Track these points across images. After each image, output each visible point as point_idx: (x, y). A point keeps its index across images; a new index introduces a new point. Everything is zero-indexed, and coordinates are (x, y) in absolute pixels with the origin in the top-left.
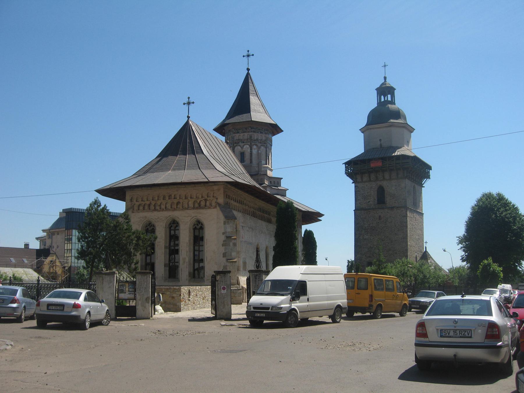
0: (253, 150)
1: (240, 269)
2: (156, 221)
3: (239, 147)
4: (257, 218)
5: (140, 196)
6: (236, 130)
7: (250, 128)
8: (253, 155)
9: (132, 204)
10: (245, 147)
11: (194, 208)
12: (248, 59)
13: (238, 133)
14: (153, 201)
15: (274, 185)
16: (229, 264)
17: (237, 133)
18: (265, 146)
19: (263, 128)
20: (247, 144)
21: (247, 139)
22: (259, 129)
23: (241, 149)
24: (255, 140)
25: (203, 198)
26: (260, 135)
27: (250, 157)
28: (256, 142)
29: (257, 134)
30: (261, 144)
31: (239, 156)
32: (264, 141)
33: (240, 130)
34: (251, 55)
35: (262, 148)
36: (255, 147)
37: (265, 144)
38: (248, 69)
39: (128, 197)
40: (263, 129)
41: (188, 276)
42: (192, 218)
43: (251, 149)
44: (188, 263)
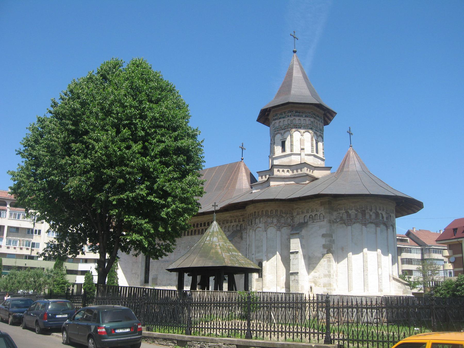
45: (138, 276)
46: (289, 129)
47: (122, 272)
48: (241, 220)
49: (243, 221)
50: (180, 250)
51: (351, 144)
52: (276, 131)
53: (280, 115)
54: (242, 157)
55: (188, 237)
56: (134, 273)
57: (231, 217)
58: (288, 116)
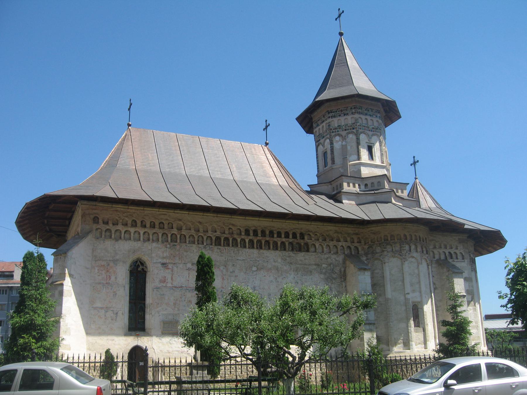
0: (335, 144)
15: (373, 188)
17: (317, 126)
18: (354, 132)
22: (342, 111)
24: (336, 129)
26: (342, 118)
28: (338, 131)
29: (339, 118)
30: (347, 131)
31: (322, 160)
32: (351, 126)
33: (319, 120)
34: (342, 13)
35: (351, 136)
36: (337, 138)
37: (353, 129)
40: (349, 108)
43: (332, 143)
45: (117, 313)
46: (379, 134)
47: (76, 303)
48: (356, 241)
49: (359, 242)
50: (234, 272)
51: (416, 176)
52: (361, 129)
53: (366, 110)
54: (267, 140)
55: (252, 250)
56: (102, 308)
57: (336, 232)
58: (377, 116)
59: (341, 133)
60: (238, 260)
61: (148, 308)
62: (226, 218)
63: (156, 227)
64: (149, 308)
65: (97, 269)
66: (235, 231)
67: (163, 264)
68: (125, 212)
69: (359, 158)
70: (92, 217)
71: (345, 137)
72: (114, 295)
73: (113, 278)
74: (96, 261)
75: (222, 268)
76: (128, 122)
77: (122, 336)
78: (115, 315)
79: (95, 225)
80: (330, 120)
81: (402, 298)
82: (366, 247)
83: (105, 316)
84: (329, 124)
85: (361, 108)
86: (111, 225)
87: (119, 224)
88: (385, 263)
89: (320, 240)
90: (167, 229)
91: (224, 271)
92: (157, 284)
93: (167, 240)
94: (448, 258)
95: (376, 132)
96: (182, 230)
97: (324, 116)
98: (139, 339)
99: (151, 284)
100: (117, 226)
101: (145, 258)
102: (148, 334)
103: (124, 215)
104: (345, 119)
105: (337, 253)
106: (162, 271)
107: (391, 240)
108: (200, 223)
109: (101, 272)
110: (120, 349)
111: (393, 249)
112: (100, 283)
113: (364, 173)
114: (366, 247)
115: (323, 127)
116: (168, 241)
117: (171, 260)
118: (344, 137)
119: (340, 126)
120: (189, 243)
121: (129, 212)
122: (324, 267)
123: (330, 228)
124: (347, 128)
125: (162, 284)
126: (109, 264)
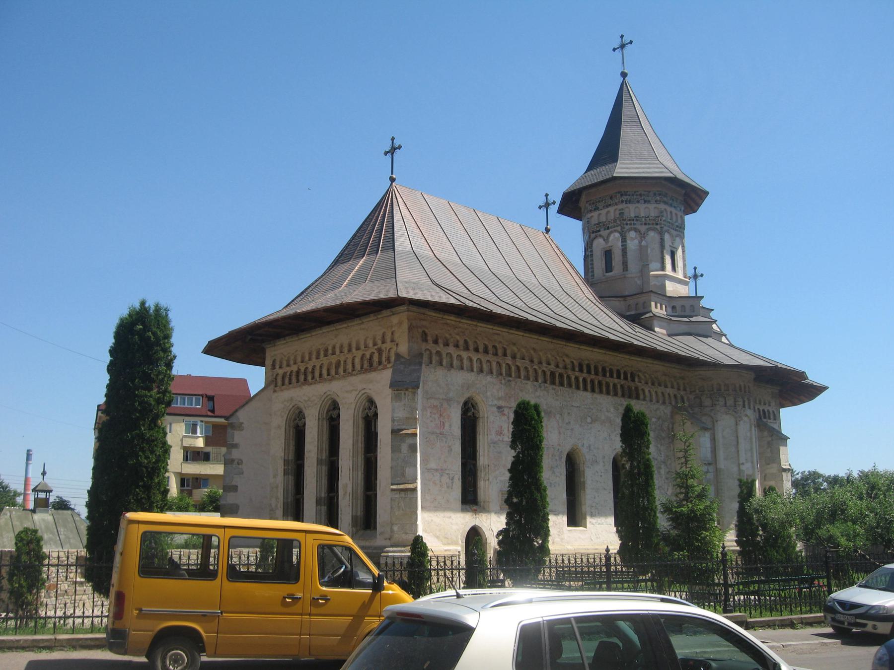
1: (489, 507)
2: (306, 405)
3: (601, 240)
4: (570, 385)
5: (285, 356)
6: (593, 203)
7: (619, 195)
8: (628, 254)
9: (273, 375)
10: (611, 237)
11: (363, 370)
12: (623, 54)
13: (597, 209)
14: (302, 364)
15: (683, 314)
16: (397, 496)
17: (595, 209)
18: (657, 229)
19: (650, 192)
20: (616, 231)
21: (615, 220)
23: (604, 242)
25: (376, 347)
27: (623, 258)
29: (637, 205)
30: (647, 227)
31: (602, 260)
32: (654, 220)
33: (599, 202)
35: (652, 234)
36: (632, 234)
37: (657, 224)
38: (624, 75)
39: (269, 362)
41: (351, 526)
42: (358, 394)
43: (624, 240)
44: (351, 496)
45: (453, 479)
48: (682, 388)
49: (685, 390)
56: (436, 470)
59: (638, 226)
60: (572, 406)
61: (482, 471)
62: (559, 344)
63: (489, 352)
64: (484, 471)
65: (429, 410)
66: (569, 364)
67: (499, 408)
68: (457, 327)
69: (663, 268)
70: (420, 330)
71: (644, 234)
72: (449, 451)
73: (447, 425)
74: (427, 399)
75: (558, 416)
76: (391, 175)
77: (459, 512)
78: (451, 481)
79: (424, 344)
80: (623, 206)
81: (735, 469)
82: (692, 397)
83: (440, 482)
84: (621, 211)
85: (666, 195)
86: (442, 346)
87: (451, 345)
88: (717, 421)
89: (650, 384)
90: (500, 356)
91: (560, 421)
92: (493, 436)
93: (500, 371)
94: (762, 418)
95: (679, 231)
96: (517, 359)
97: (611, 198)
98: (477, 516)
99: (486, 436)
100: (447, 347)
101: (478, 399)
102: (484, 508)
103: (455, 331)
104: (646, 208)
105: (664, 403)
106: (498, 418)
107: (725, 391)
108: (534, 350)
109: (434, 416)
110: (458, 530)
111: (726, 403)
112: (433, 433)
113: (669, 290)
114: (692, 397)
115: (608, 212)
116: (501, 374)
117: (508, 402)
118: (643, 234)
119: (638, 217)
120: (524, 379)
121: (460, 327)
122: (653, 422)
123: (658, 367)
124: (648, 221)
125: (499, 437)
126: (442, 405)
